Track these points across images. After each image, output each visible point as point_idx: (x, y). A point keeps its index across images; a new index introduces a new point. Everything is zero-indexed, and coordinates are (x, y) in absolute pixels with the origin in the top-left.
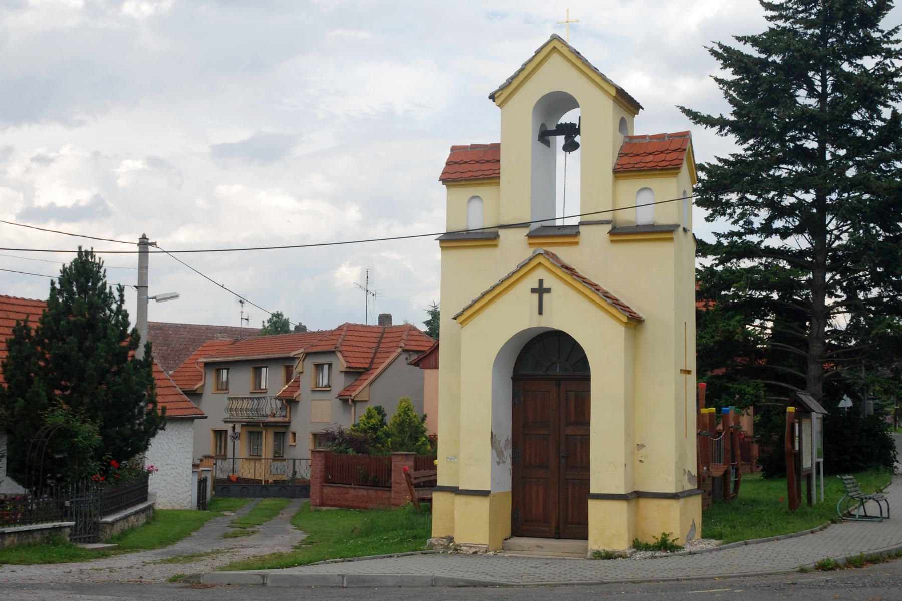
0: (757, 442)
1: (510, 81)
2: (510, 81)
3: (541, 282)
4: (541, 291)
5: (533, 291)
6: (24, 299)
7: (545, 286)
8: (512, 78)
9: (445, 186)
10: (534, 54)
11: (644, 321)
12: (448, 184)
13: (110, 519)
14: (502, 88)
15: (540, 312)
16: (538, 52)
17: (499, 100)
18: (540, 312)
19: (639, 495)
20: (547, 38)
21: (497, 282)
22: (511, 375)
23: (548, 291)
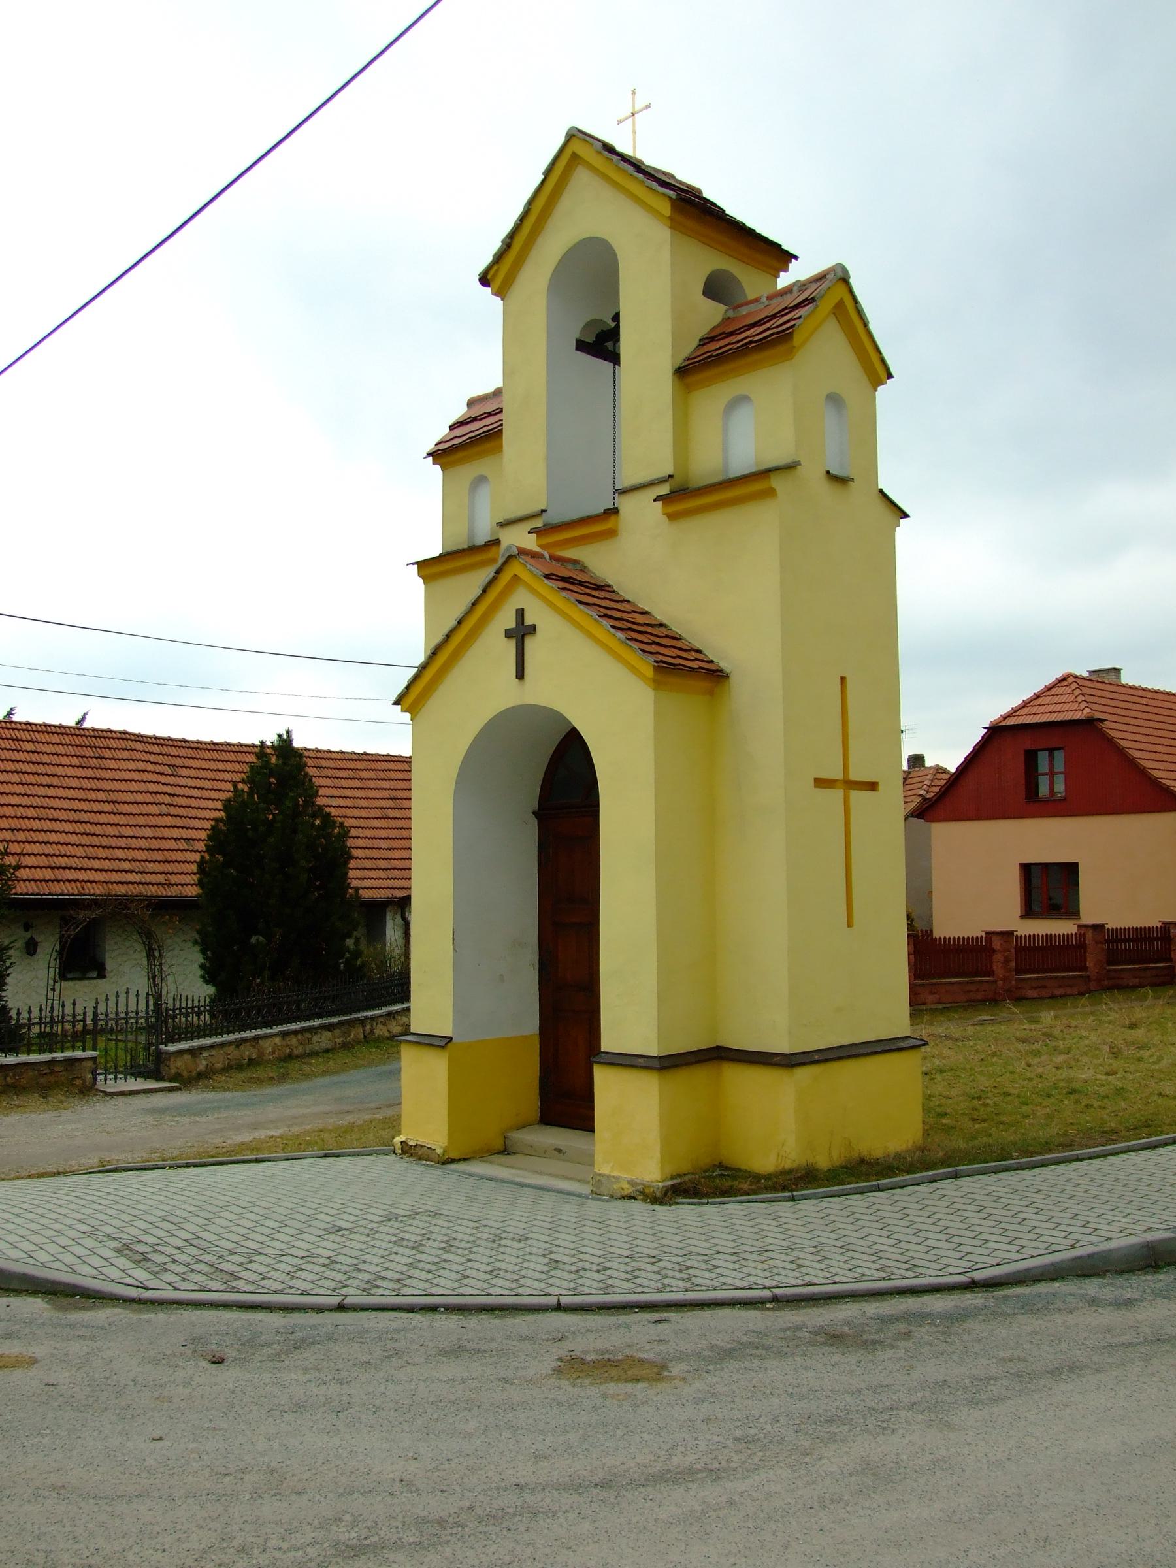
0: (994, 951)
1: (508, 240)
2: (508, 240)
3: (521, 613)
4: (521, 632)
5: (509, 634)
6: (342, 752)
7: (528, 621)
8: (512, 235)
9: (438, 467)
10: (543, 177)
11: (727, 676)
12: (444, 460)
13: (171, 1048)
14: (499, 258)
15: (520, 674)
16: (548, 173)
17: (497, 283)
18: (520, 674)
19: (719, 1055)
20: (561, 140)
21: (452, 623)
22: (536, 805)
23: (533, 629)
